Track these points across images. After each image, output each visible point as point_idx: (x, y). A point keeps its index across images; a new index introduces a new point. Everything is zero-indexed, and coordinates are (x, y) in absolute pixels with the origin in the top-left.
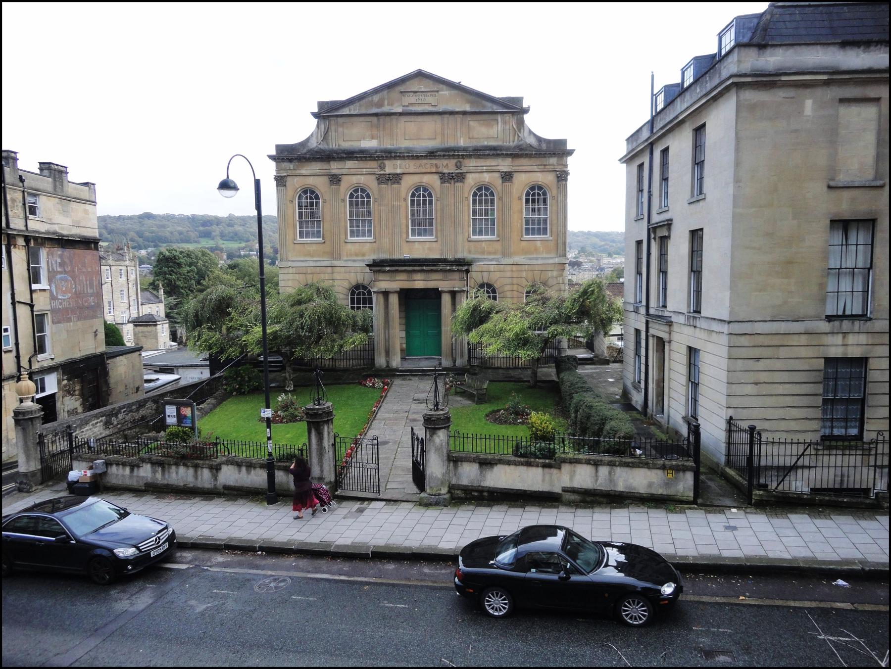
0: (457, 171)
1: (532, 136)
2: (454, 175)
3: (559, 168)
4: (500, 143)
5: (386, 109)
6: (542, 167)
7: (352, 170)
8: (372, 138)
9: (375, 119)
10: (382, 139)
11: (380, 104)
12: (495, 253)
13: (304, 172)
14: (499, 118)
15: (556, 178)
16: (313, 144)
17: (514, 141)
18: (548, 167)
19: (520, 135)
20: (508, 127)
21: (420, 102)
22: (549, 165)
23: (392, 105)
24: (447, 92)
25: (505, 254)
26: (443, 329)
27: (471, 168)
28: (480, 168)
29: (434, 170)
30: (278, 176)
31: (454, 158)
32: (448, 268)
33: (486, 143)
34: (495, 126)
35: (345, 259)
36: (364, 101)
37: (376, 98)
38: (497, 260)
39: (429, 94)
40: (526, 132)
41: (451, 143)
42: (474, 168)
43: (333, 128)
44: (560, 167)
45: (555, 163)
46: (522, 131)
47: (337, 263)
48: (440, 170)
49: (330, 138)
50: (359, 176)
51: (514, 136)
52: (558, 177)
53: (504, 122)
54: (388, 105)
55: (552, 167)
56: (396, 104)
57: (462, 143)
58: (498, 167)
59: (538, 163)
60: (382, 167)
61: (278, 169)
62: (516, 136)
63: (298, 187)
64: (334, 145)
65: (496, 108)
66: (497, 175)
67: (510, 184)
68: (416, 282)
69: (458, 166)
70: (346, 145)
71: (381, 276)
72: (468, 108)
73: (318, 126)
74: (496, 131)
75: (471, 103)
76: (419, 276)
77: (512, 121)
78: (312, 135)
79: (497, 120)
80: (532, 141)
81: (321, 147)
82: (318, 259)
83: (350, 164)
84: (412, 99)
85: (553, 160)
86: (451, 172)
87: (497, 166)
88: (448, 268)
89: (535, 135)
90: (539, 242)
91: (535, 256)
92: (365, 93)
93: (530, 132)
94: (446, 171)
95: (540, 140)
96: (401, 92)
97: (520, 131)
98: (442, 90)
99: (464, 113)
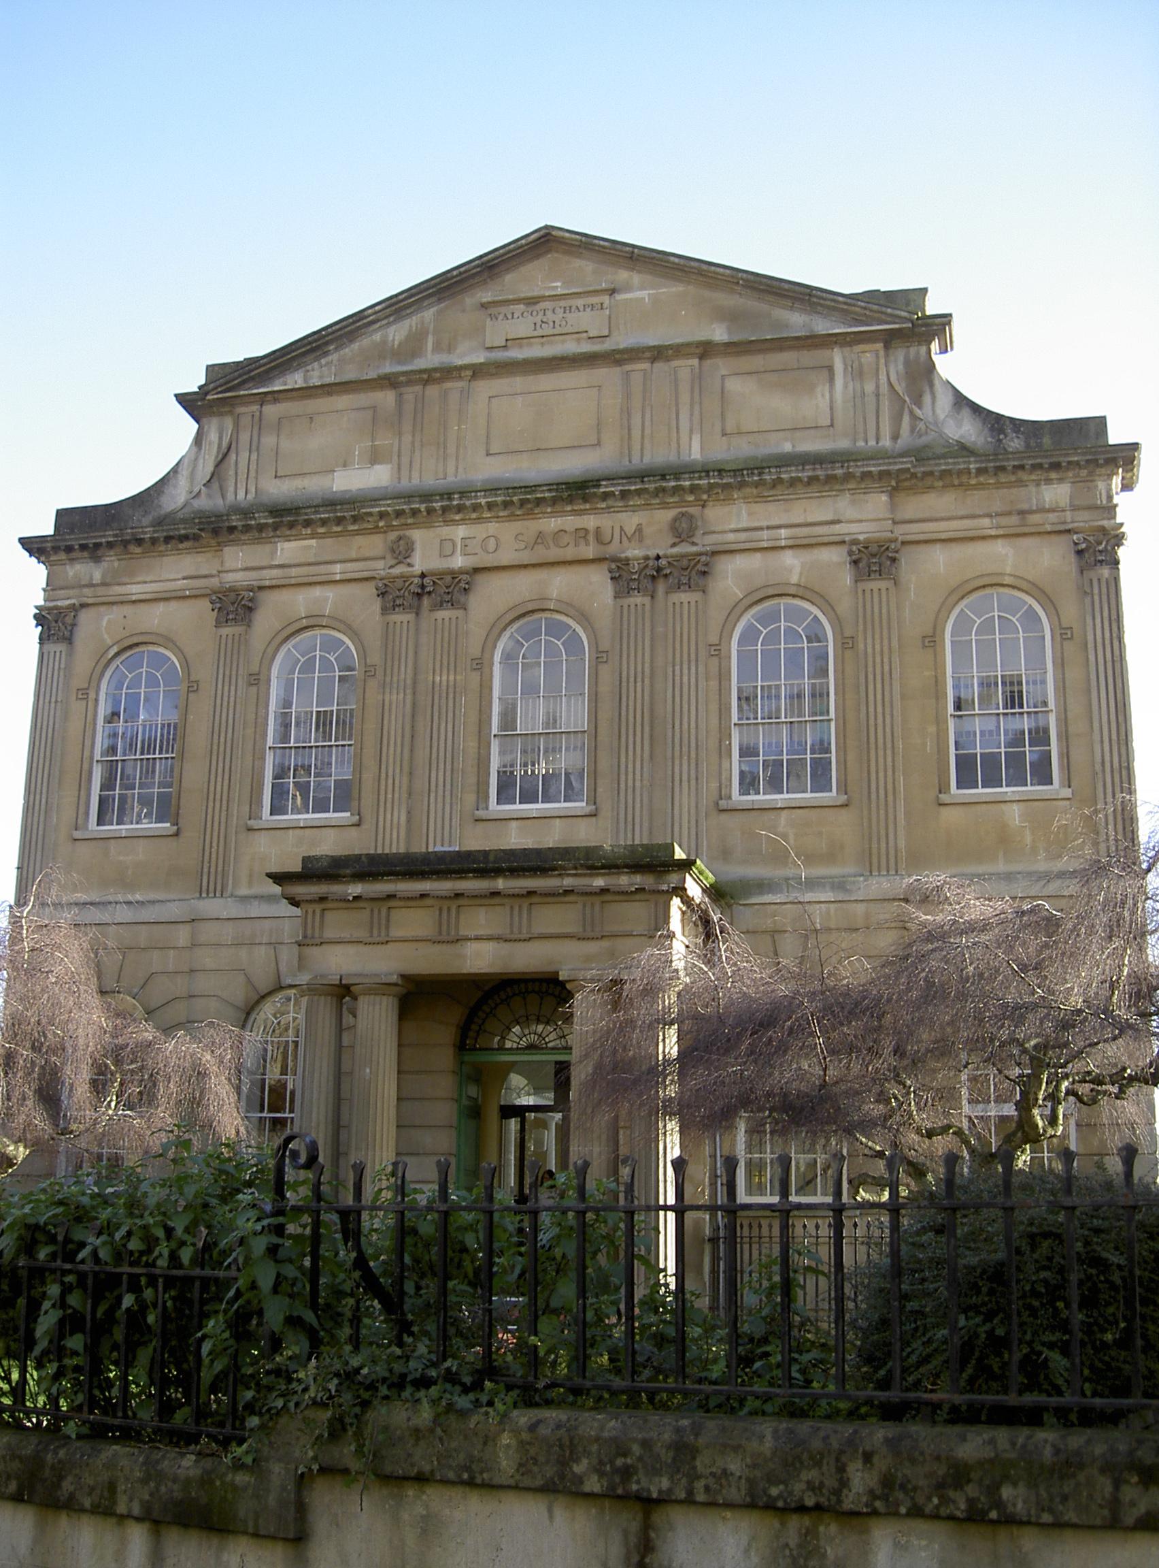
0: (675, 550)
1: (966, 412)
2: (663, 562)
3: (1083, 520)
4: (843, 444)
5: (430, 359)
6: (1014, 520)
7: (294, 572)
8: (375, 458)
9: (386, 398)
10: (405, 460)
11: (414, 346)
12: (830, 857)
13: (135, 590)
14: (838, 358)
15: (1073, 558)
16: (176, 499)
17: (895, 437)
18: (1035, 518)
19: (918, 412)
20: (869, 387)
21: (548, 330)
22: (1042, 510)
23: (450, 349)
24: (644, 294)
25: (871, 863)
26: (531, 1103)
27: (731, 537)
28: (765, 534)
29: (589, 551)
30: (49, 609)
31: (665, 506)
32: (599, 882)
33: (787, 447)
34: (822, 390)
35: (243, 891)
36: (355, 346)
37: (397, 333)
38: (840, 885)
39: (580, 302)
40: (944, 403)
41: (657, 455)
42: (743, 536)
43: (244, 437)
44: (1085, 515)
45: (1064, 501)
46: (927, 399)
47: (212, 906)
48: (613, 549)
49: (232, 472)
50: (317, 592)
51: (897, 420)
52: (1080, 553)
53: (857, 373)
54: (437, 348)
55: (1052, 517)
56: (461, 349)
57: (695, 452)
58: (837, 528)
59: (997, 506)
60: (402, 551)
61: (52, 587)
62: (906, 419)
63: (109, 642)
64: (241, 495)
65: (823, 326)
66: (835, 556)
67: (883, 585)
68: (471, 948)
69: (682, 530)
70: (279, 489)
71: (336, 923)
72: (719, 334)
73: (198, 440)
74: (824, 403)
75: (732, 317)
76: (480, 920)
77: (893, 368)
78: (175, 470)
79: (830, 369)
80: (966, 430)
81: (203, 503)
82: (152, 896)
83: (288, 550)
84: (521, 326)
85: (1057, 493)
86: (652, 553)
87: (839, 522)
88: (599, 882)
89: (976, 409)
90: (1015, 807)
91: (1001, 867)
92: (359, 315)
93: (961, 401)
94: (634, 552)
95: (996, 423)
96: (484, 306)
97: (918, 401)
98: (628, 288)
99: (706, 350)
